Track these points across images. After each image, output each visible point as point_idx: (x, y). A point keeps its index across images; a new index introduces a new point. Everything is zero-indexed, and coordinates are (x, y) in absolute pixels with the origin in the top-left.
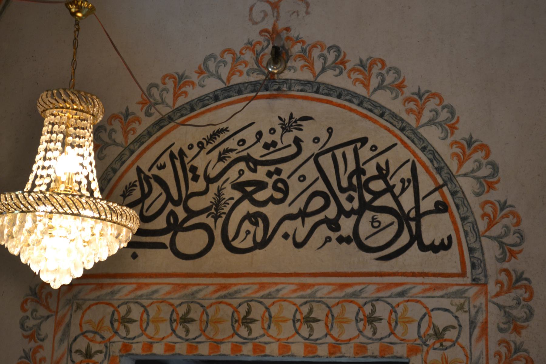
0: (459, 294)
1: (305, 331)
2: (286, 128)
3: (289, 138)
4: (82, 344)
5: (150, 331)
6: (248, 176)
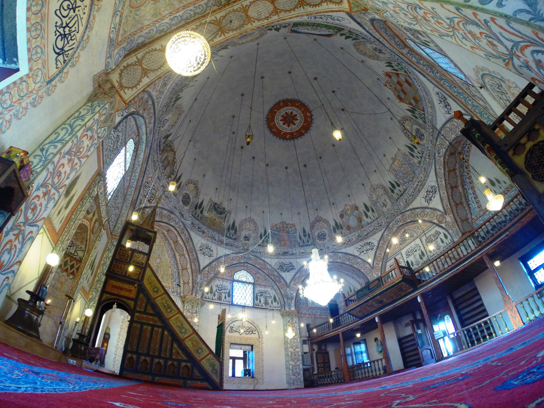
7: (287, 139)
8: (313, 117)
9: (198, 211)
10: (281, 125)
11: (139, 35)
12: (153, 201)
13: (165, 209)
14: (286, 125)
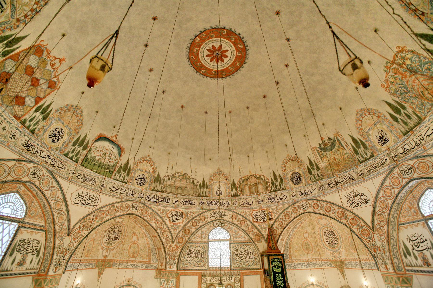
7: (245, 46)
8: (198, 33)
9: (315, 172)
10: (228, 59)
11: (150, 245)
12: (273, 216)
13: (287, 208)
14: (226, 54)
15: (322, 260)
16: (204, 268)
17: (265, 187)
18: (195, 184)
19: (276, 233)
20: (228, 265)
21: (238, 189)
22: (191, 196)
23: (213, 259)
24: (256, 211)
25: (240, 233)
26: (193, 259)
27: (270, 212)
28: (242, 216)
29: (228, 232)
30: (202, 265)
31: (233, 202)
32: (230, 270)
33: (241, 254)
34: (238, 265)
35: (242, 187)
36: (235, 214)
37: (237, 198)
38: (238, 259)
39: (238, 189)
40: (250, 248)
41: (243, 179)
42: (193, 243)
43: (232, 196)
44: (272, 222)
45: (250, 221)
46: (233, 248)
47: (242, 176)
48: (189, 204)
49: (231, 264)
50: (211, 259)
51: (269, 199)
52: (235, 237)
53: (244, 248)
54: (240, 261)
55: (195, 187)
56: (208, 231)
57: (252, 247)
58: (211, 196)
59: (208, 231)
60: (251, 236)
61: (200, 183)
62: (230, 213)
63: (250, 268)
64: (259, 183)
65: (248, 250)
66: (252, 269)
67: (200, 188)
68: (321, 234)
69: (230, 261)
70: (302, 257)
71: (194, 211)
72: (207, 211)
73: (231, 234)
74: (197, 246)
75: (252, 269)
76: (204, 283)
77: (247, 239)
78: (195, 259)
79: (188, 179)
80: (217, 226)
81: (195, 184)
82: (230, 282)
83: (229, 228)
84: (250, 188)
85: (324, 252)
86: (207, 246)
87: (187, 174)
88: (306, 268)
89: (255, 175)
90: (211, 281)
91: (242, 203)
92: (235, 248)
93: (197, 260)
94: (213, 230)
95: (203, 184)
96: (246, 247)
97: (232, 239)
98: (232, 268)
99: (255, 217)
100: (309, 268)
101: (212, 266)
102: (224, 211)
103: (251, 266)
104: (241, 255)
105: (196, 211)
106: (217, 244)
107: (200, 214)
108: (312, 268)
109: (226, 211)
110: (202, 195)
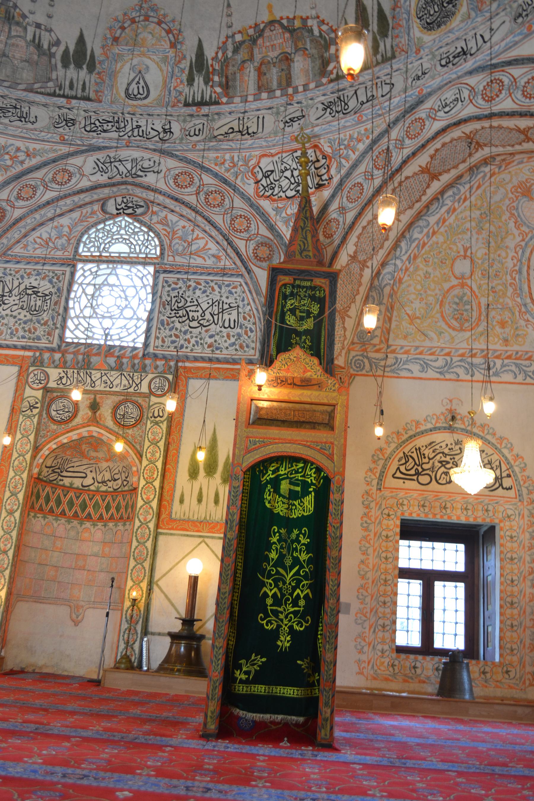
0: (515, 504)
1: (465, 513)
2: (456, 444)
3: (457, 447)
4: (386, 511)
5: (411, 508)
6: (443, 459)
12: (333, 171)
15: (509, 357)
16: (43, 343)
17: (318, 62)
18: (46, 46)
19: (334, 229)
20: (140, 343)
21: (216, 78)
22: (25, 90)
23: (84, 317)
24: (272, 155)
25: (201, 243)
26: (8, 312)
27: (325, 157)
28: (216, 175)
29: (157, 235)
30: (40, 332)
31: (192, 124)
32: (141, 355)
33: (193, 308)
34: (173, 342)
35: (231, 69)
36: (190, 168)
37: (205, 110)
38: (178, 325)
39: (216, 78)
40: (231, 292)
41: (238, 38)
42: (18, 262)
43: (187, 104)
44: (326, 193)
45: (243, 196)
46: (168, 289)
47: (237, 27)
48: (12, 119)
49: (147, 338)
50: (77, 317)
51: (327, 107)
52: (181, 255)
53: (209, 291)
54: (185, 333)
55: (46, 58)
56: (79, 228)
57: (239, 290)
58: (107, 97)
59: (79, 228)
60: (241, 245)
61: (67, 48)
62: (171, 163)
63: (218, 354)
64: (297, 50)
65: (224, 299)
66: (227, 362)
67: (66, 65)
68: (525, 269)
69: (148, 331)
70: (431, 339)
71: (32, 146)
72: (83, 152)
73: (166, 241)
74: (29, 274)
75: (227, 362)
76: (35, 386)
77: (226, 263)
78: (14, 314)
79: (18, 24)
80: (118, 214)
81: (46, 46)
82: (131, 390)
83: (164, 222)
84: (260, 73)
85: (520, 333)
86: (68, 274)
87: (15, 6)
88: (438, 376)
89: (285, 22)
90: (64, 381)
91: (225, 129)
92: (173, 289)
93: (21, 316)
94: (100, 227)
95: (76, 52)
96: (216, 287)
97: (169, 259)
98: (151, 350)
99: (264, 182)
100: (453, 376)
101: (76, 341)
102: (147, 155)
103: (225, 352)
104: (191, 314)
105: (38, 147)
106: (109, 271)
107: (54, 161)
108: (463, 376)
109: (156, 157)
110: (67, 91)
